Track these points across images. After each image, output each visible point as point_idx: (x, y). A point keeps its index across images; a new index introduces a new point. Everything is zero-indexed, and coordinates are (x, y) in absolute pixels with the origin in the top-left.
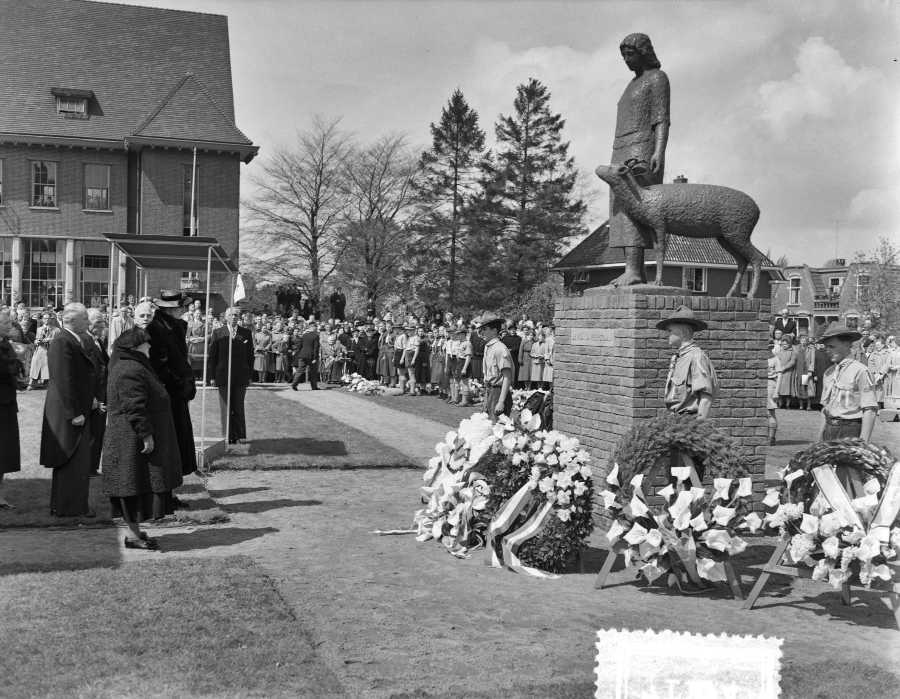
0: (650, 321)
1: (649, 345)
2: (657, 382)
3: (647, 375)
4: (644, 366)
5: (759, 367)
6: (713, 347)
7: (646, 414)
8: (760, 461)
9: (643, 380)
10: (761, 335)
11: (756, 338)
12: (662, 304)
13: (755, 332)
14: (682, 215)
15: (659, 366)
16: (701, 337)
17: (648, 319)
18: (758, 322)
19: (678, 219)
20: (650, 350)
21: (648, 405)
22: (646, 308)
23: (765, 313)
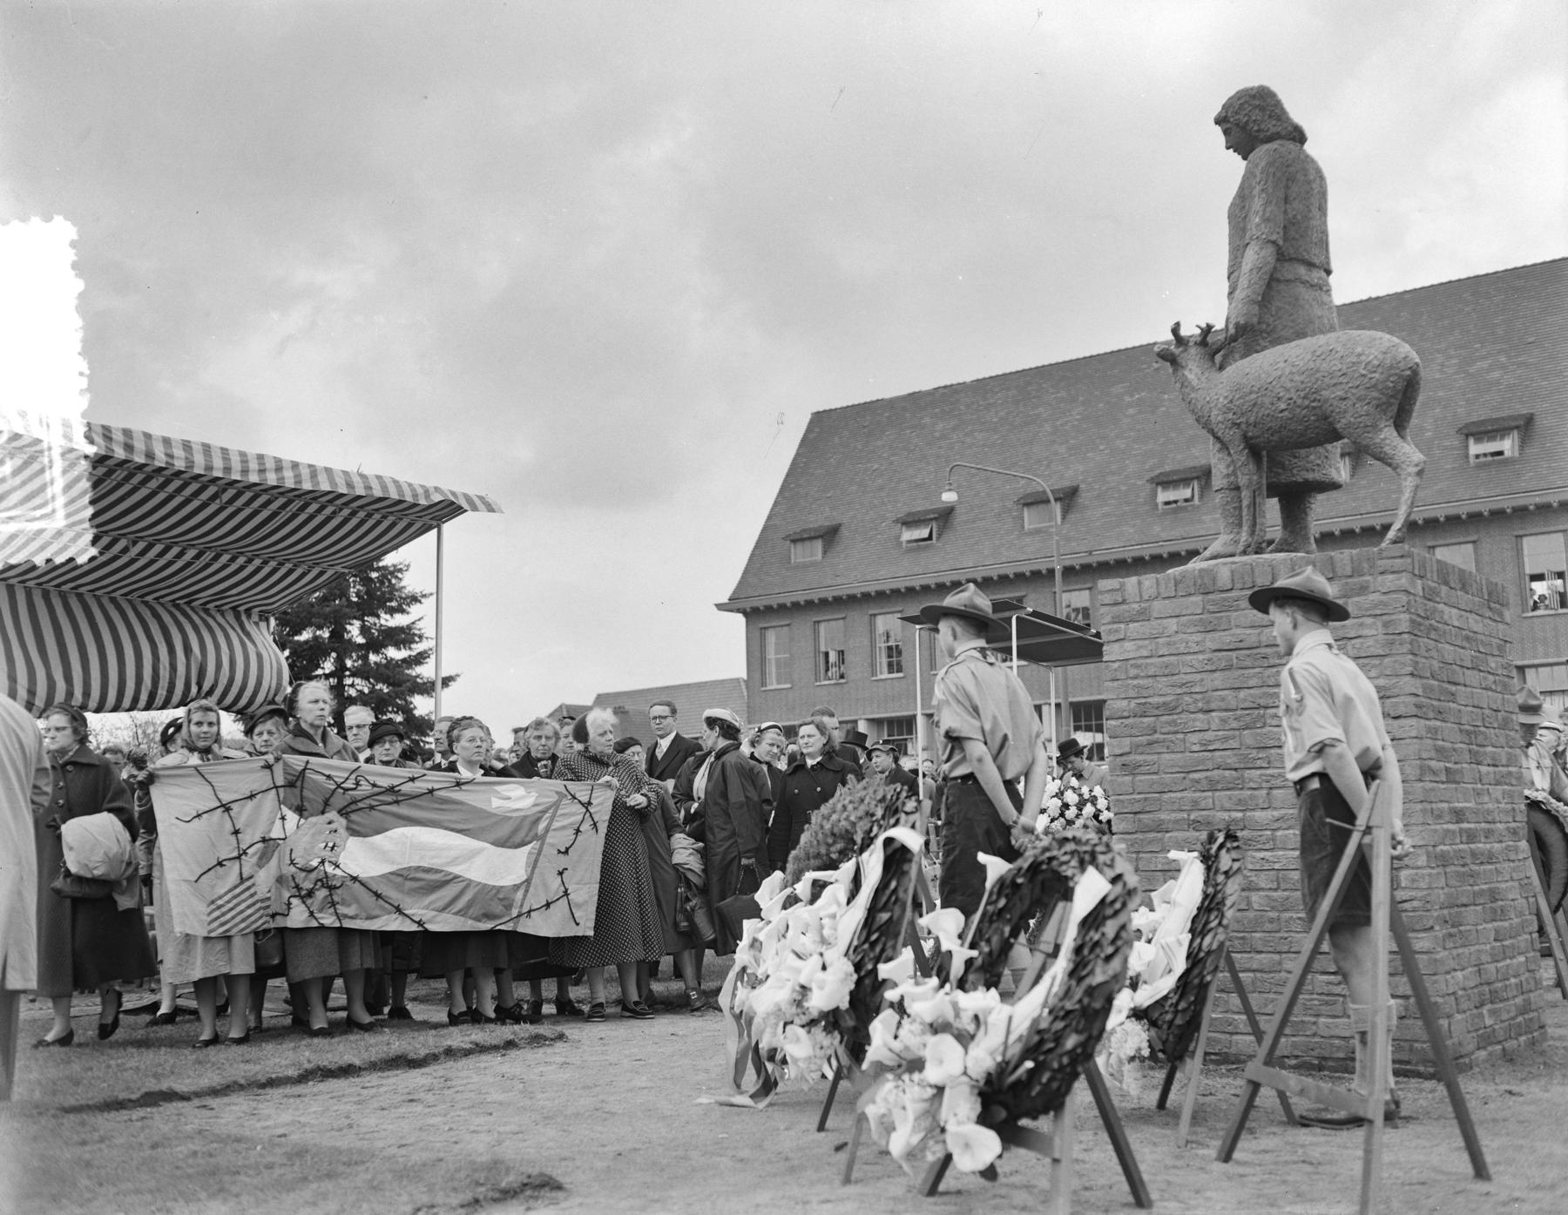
0: (1131, 625)
1: (1133, 672)
2: (1156, 742)
3: (1133, 731)
4: (1126, 714)
5: (1388, 694)
6: (1272, 662)
7: (1137, 808)
8: (1416, 904)
9: (1127, 741)
10: (1386, 625)
11: (1373, 632)
12: (1153, 591)
13: (1369, 621)
14: (1255, 410)
15: (1157, 712)
16: (1241, 645)
17: (1127, 623)
18: (1372, 597)
19: (1252, 420)
20: (1135, 682)
21: (1139, 790)
22: (1124, 602)
23: (1391, 577)
